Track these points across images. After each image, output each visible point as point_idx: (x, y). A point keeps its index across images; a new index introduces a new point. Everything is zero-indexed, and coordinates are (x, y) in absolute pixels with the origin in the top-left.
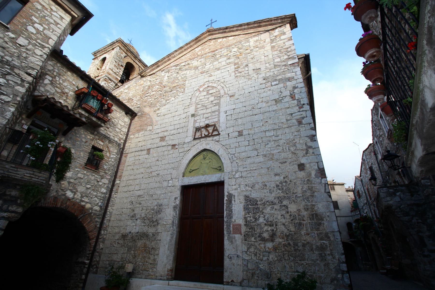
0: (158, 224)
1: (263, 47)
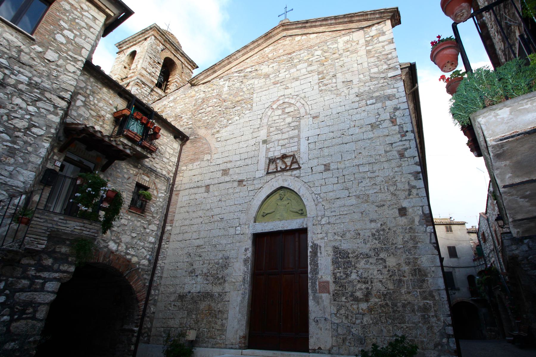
0: (225, 281)
1: (356, 51)
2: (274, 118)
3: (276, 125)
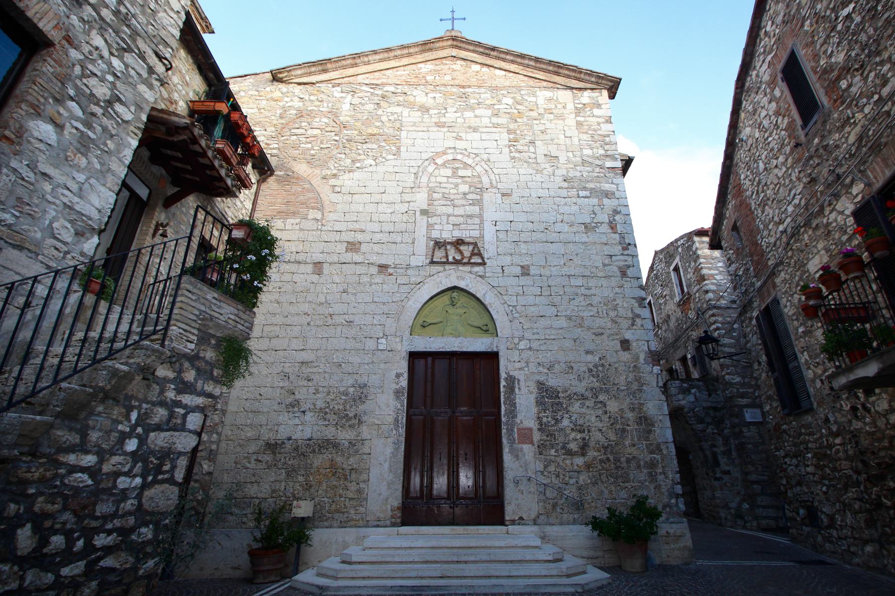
1: (561, 117)
2: (439, 179)
3: (443, 190)
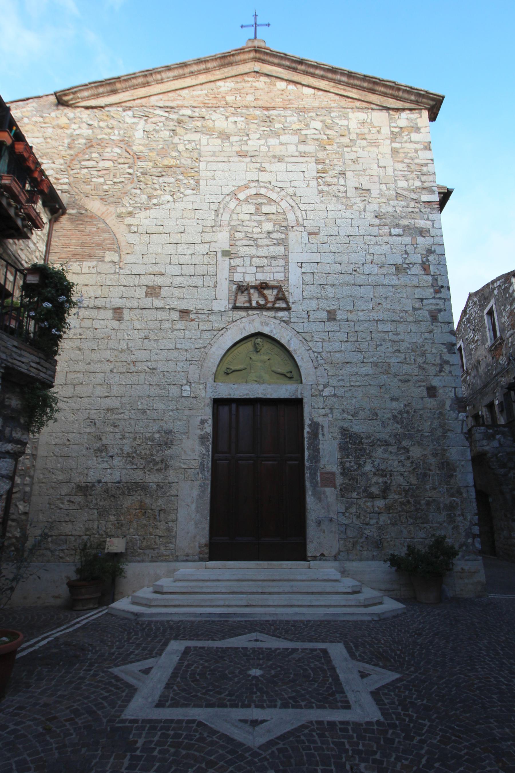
1: (375, 144)
2: (242, 217)
